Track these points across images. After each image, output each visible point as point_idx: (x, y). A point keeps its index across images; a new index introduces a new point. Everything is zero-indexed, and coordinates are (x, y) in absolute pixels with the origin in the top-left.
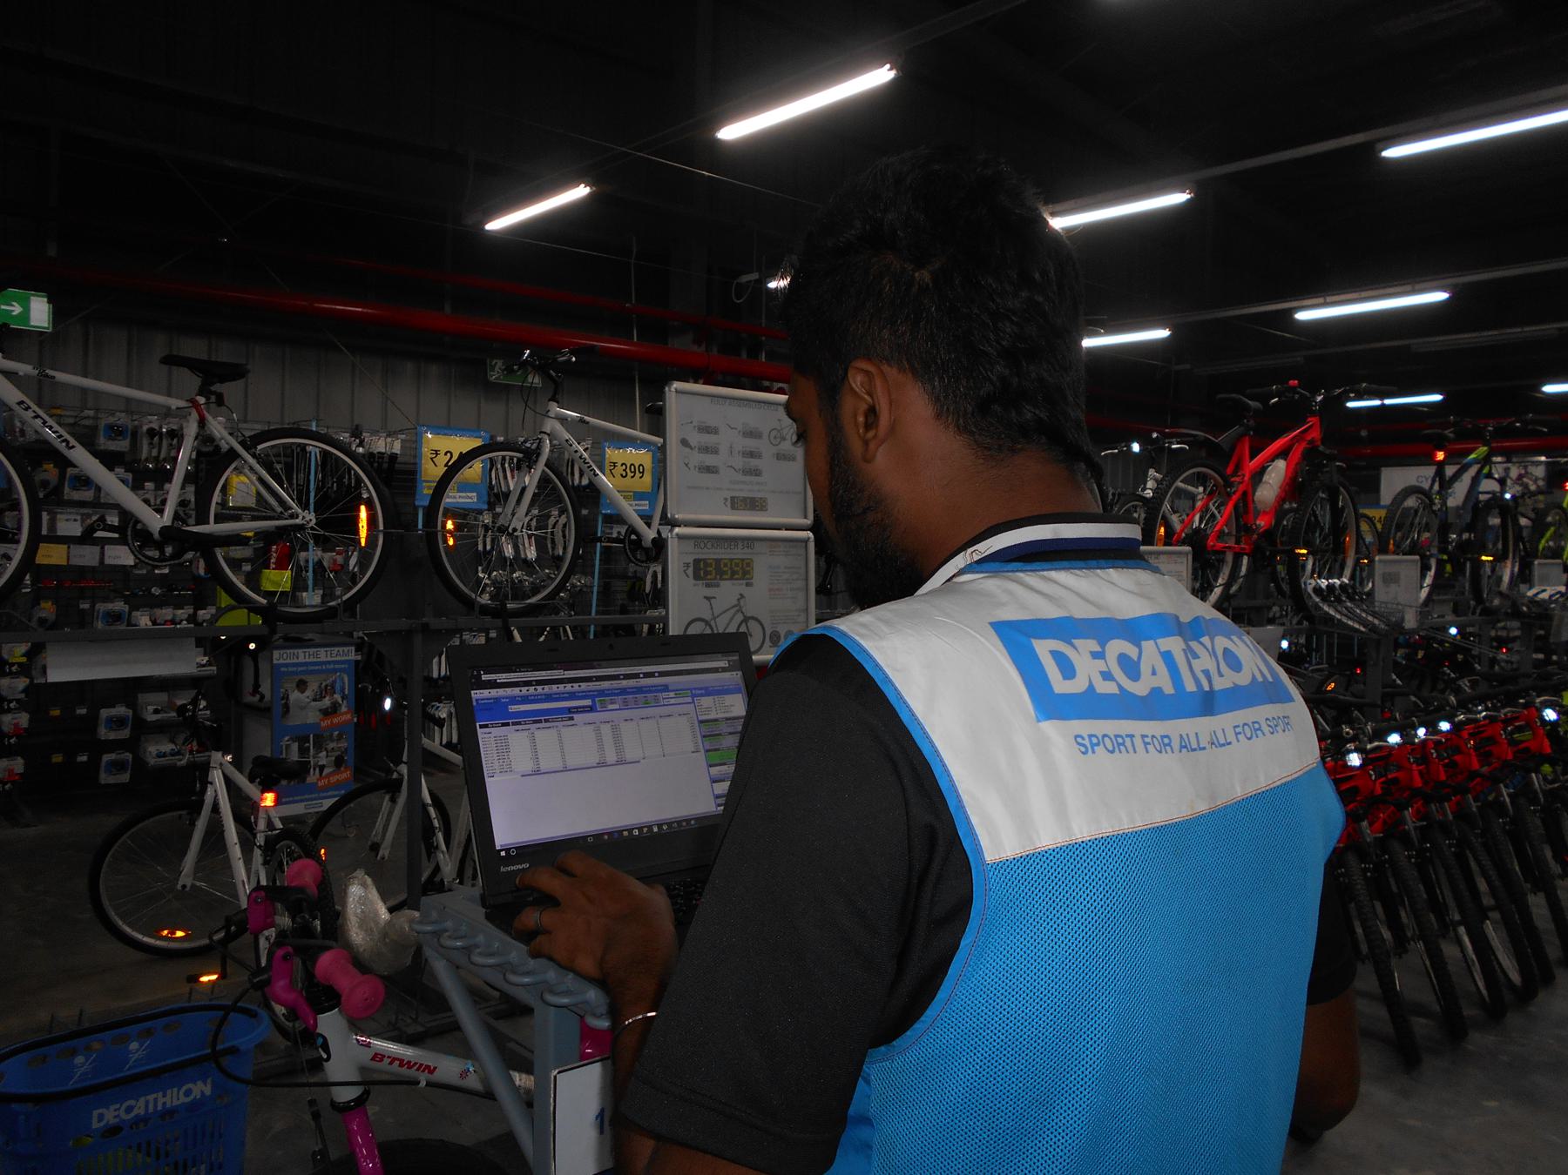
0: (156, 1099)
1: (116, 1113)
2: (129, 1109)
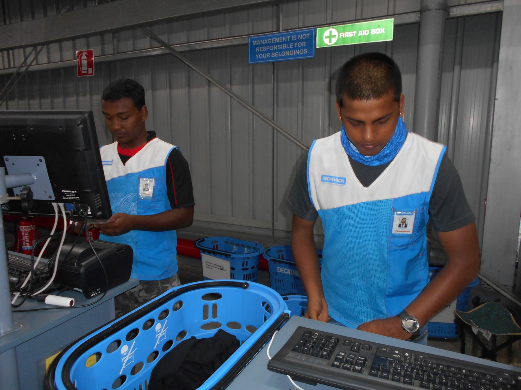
0: (334, 179)
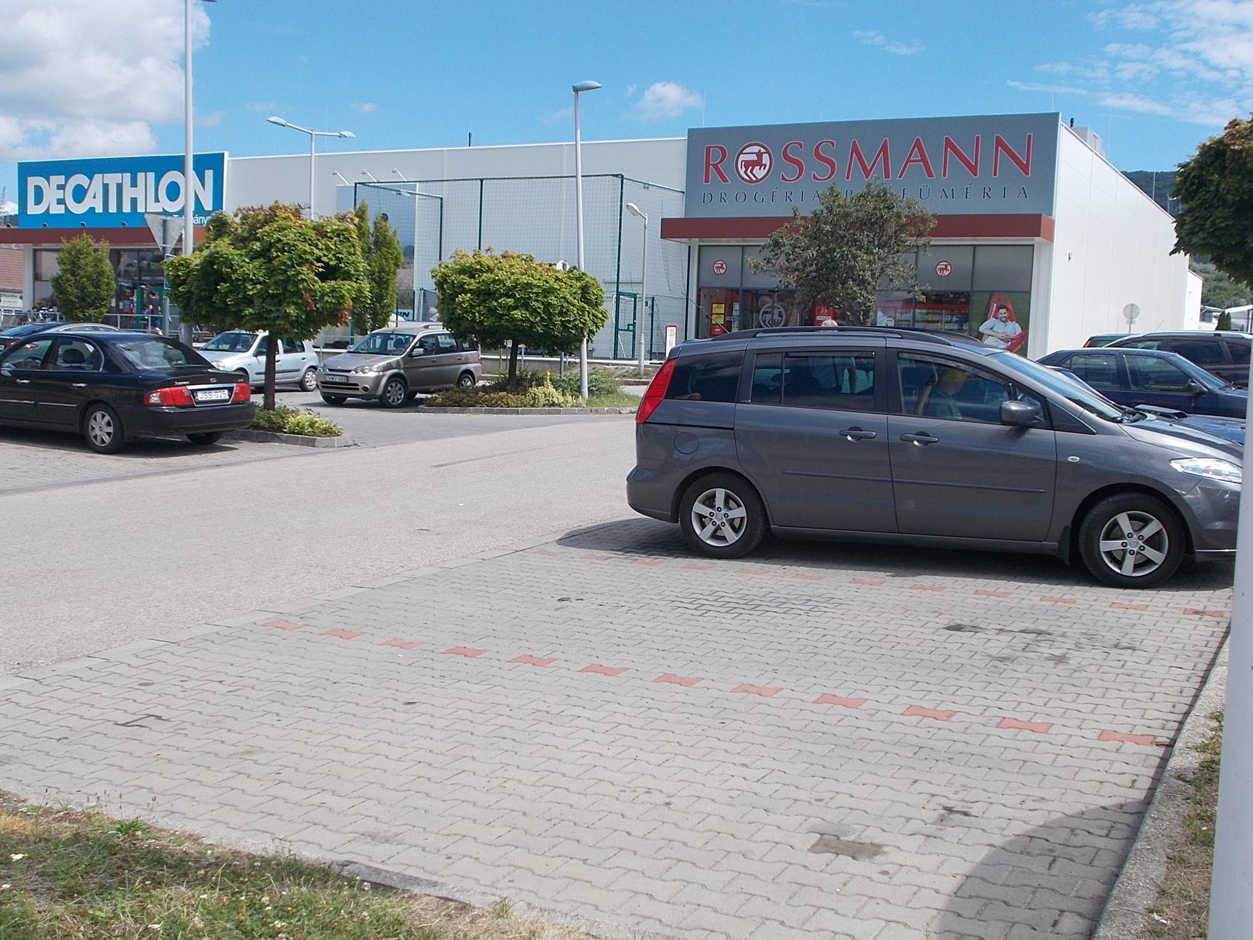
0: (120, 187)
2: (80, 194)
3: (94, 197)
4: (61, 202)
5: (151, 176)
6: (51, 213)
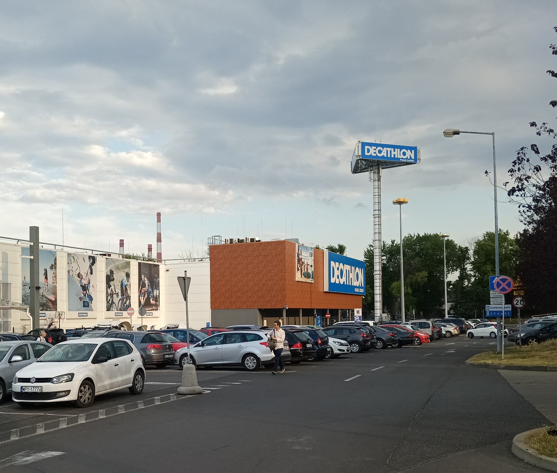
0: (391, 151)
1: (375, 151)
2: (380, 152)
3: (384, 153)
4: (375, 153)
5: (399, 150)
6: (372, 155)
